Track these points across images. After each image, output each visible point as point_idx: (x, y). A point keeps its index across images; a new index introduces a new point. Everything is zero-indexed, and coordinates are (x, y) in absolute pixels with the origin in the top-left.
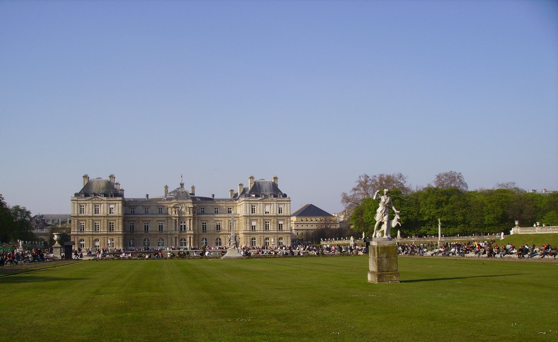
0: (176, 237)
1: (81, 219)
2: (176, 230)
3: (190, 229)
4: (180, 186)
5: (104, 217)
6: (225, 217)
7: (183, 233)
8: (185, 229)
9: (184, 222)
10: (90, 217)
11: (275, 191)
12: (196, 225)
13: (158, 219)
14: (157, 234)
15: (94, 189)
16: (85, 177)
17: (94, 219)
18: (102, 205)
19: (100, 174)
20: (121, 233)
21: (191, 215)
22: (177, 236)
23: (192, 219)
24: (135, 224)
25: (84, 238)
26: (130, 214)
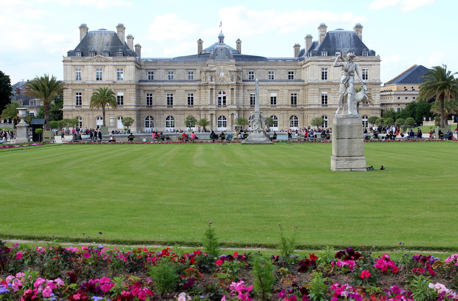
0: (212, 114)
1: (77, 87)
2: (211, 104)
3: (232, 103)
4: (217, 40)
6: (284, 85)
7: (222, 108)
8: (224, 102)
9: (224, 93)
10: (89, 85)
11: (359, 48)
12: (241, 98)
13: (186, 88)
14: (185, 110)
15: (96, 45)
16: (83, 27)
18: (107, 68)
19: (103, 23)
20: (133, 107)
21: (234, 82)
22: (214, 113)
23: (235, 87)
24: (153, 96)
26: (146, 81)
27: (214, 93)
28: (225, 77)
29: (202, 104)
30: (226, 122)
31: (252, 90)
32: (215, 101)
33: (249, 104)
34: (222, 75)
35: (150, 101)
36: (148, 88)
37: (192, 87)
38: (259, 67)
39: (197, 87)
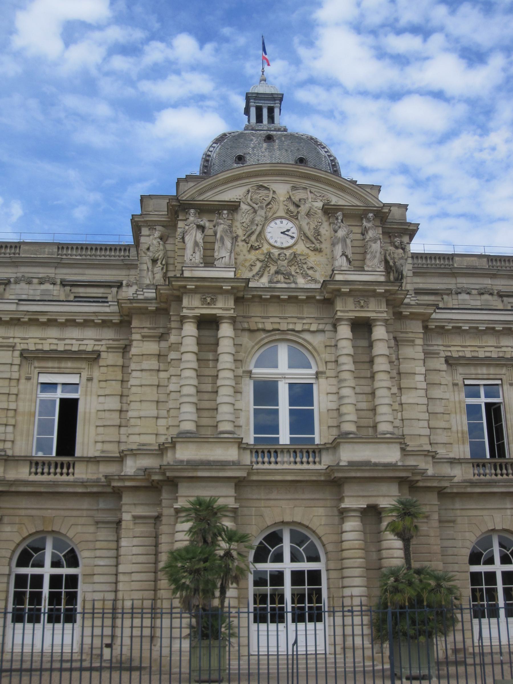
8: (302, 421)
27: (226, 346)
28: (301, 248)
29: (134, 441)
30: (315, 577)
31: (474, 362)
32: (238, 410)
37: (75, 333)
38: (463, 282)
39: (109, 334)
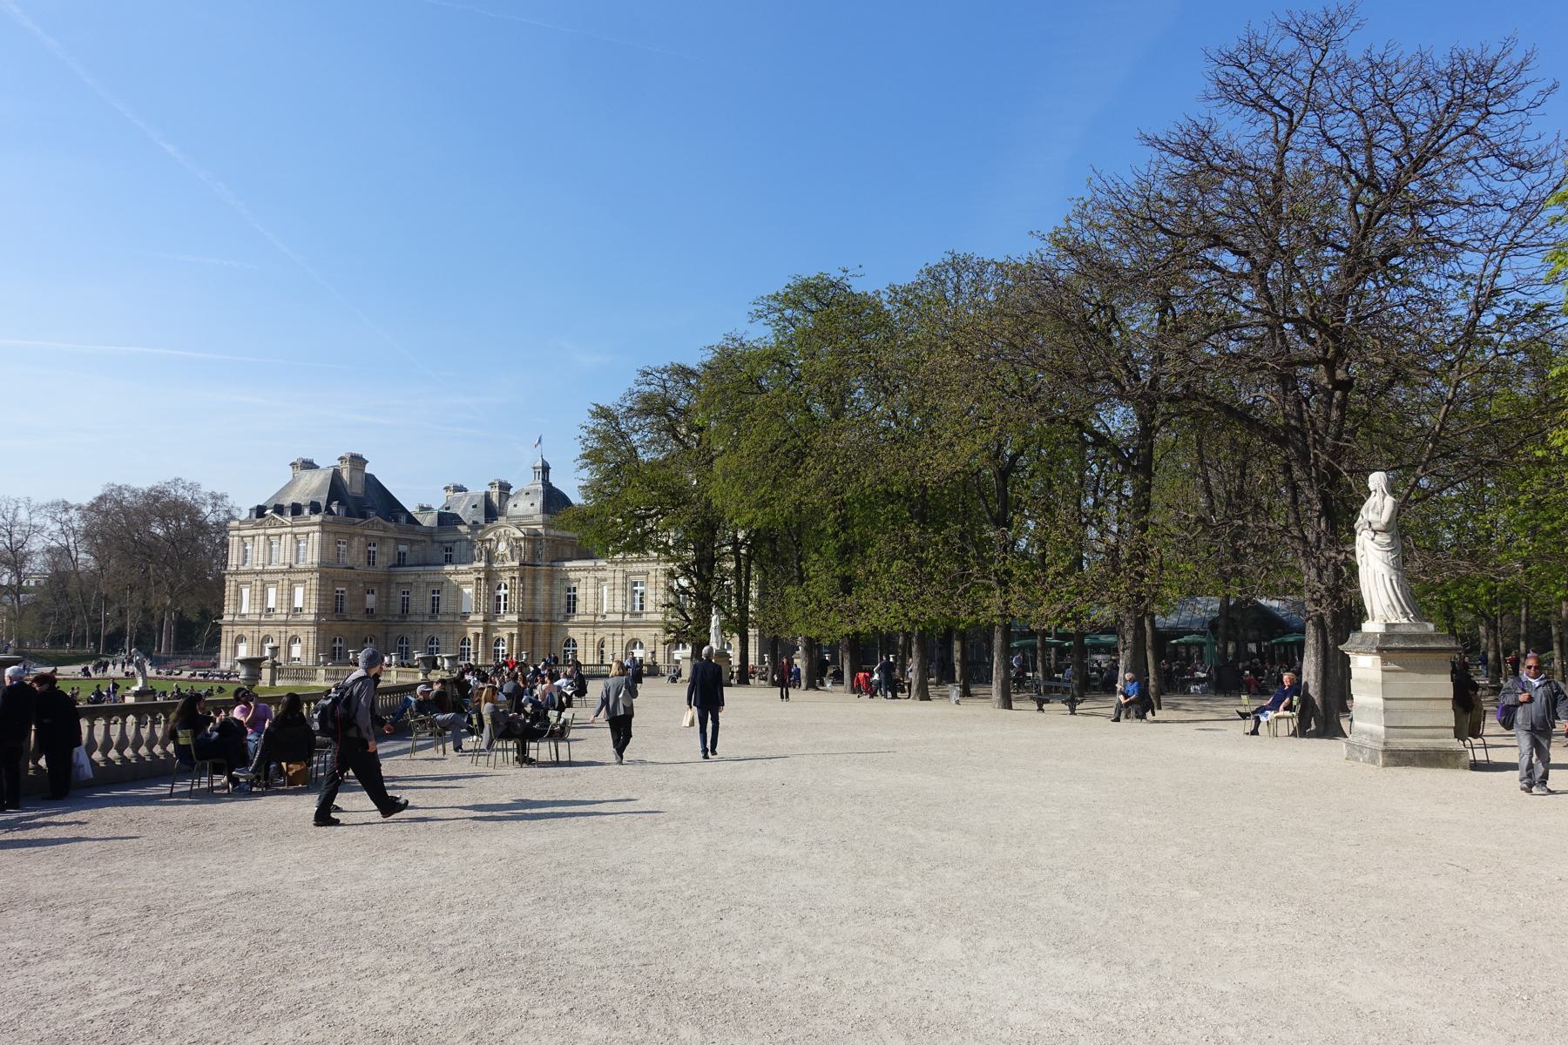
0: (477, 635)
5: (282, 572)
10: (257, 573)
17: (266, 577)
21: (516, 563)
23: (516, 574)
25: (246, 632)
33: (564, 610)
34: (502, 547)
35: (405, 604)
36: (402, 579)
